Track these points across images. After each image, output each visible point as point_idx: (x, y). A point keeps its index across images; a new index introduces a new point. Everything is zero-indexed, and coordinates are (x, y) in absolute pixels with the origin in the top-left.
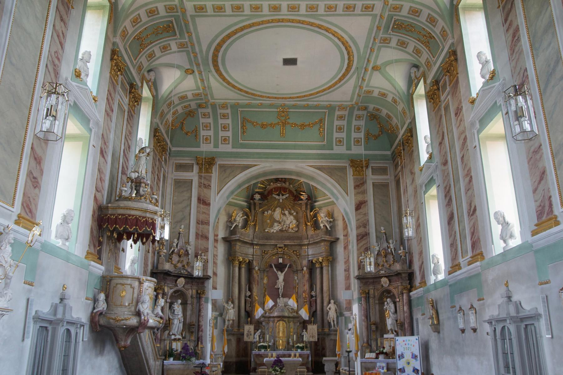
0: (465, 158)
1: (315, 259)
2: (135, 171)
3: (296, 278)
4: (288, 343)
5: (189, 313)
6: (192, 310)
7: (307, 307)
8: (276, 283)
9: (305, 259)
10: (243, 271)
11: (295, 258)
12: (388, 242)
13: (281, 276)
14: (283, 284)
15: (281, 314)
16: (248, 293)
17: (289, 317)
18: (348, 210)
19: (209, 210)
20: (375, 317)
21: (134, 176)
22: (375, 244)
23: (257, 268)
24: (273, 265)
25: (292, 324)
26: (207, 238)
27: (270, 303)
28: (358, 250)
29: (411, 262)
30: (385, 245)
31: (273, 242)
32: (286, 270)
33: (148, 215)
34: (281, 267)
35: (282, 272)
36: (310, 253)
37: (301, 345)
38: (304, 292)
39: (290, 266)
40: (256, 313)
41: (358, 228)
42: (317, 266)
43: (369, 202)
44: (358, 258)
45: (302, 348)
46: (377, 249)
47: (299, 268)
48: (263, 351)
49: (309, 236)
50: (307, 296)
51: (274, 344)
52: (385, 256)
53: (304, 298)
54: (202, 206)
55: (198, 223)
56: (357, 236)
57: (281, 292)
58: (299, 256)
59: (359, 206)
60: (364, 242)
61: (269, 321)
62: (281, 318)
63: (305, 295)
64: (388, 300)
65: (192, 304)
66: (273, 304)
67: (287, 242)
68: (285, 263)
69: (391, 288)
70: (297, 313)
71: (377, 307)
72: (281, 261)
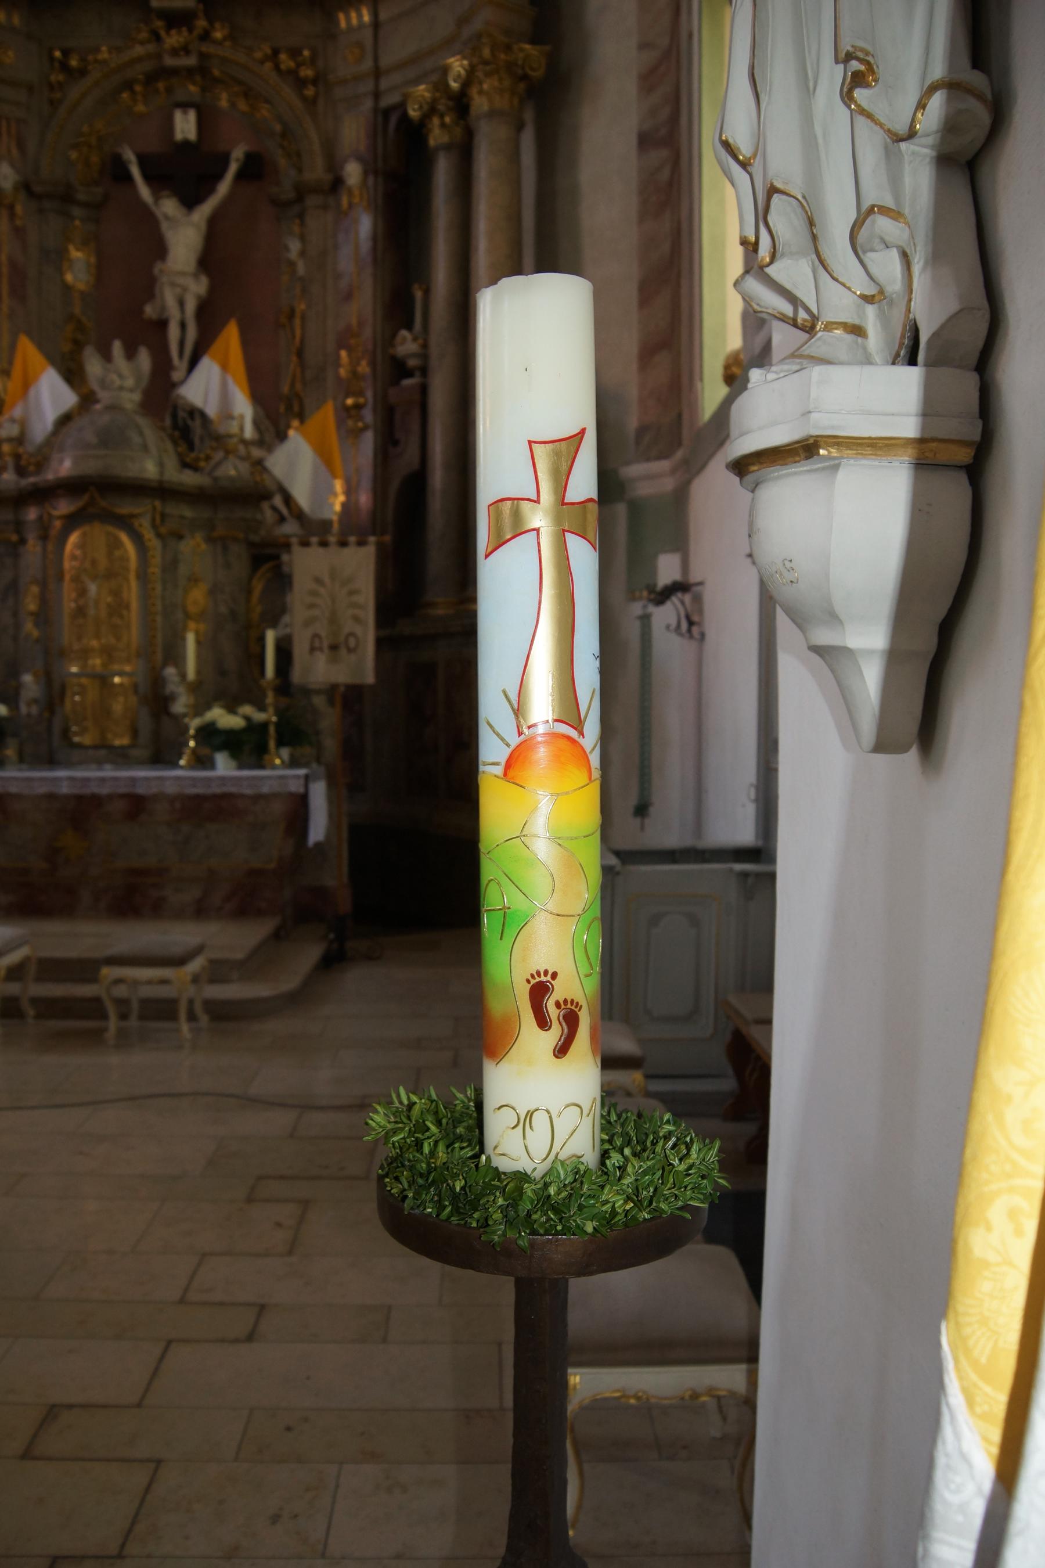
1: (422, 90)
3: (294, 246)
8: (149, 289)
13: (184, 236)
14: (198, 287)
15: (91, 467)
17: (163, 491)
24: (130, 156)
25: (194, 549)
32: (224, 188)
34: (186, 173)
35: (190, 202)
39: (254, 169)
42: (437, 136)
50: (364, 368)
61: (19, 526)
62: (100, 496)
63: (354, 363)
66: (69, 398)
72: (185, 126)
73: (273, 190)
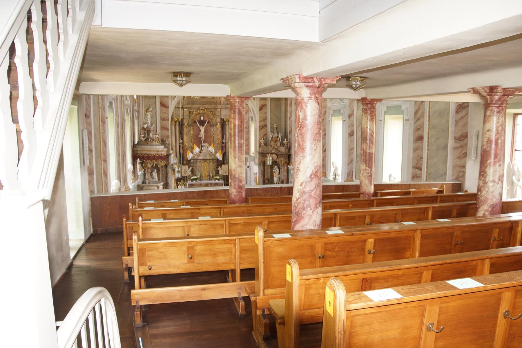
0: (324, 121)
2: (145, 123)
4: (209, 175)
5: (161, 176)
6: (162, 174)
7: (220, 151)
8: (199, 134)
9: (218, 117)
10: (177, 126)
11: (211, 116)
12: (278, 133)
13: (202, 129)
16: (181, 141)
18: (254, 109)
19: (168, 111)
20: (268, 176)
21: (145, 126)
22: (270, 133)
23: (186, 124)
25: (211, 164)
26: (168, 129)
27: (197, 150)
28: (260, 135)
29: (289, 149)
30: (276, 135)
31: (197, 106)
32: (206, 124)
33: (159, 153)
34: (202, 123)
35: (203, 126)
36: (222, 114)
37: (218, 178)
38: (218, 139)
39: (208, 122)
40: (188, 157)
41: (260, 122)
43: (267, 106)
44: (260, 140)
45: (218, 180)
46: (271, 136)
47: (215, 123)
48: (194, 182)
49: (222, 102)
51: (201, 176)
52: (276, 142)
53: (218, 144)
54: (163, 108)
55: (161, 119)
56: (260, 127)
57: (202, 139)
58: (214, 115)
59: (261, 109)
60: (263, 130)
62: (205, 160)
64: (276, 167)
65: (162, 171)
67: (207, 106)
68: (205, 120)
69: (277, 160)
70: (215, 156)
71: (269, 170)
72: (202, 118)
73: (211, 124)
